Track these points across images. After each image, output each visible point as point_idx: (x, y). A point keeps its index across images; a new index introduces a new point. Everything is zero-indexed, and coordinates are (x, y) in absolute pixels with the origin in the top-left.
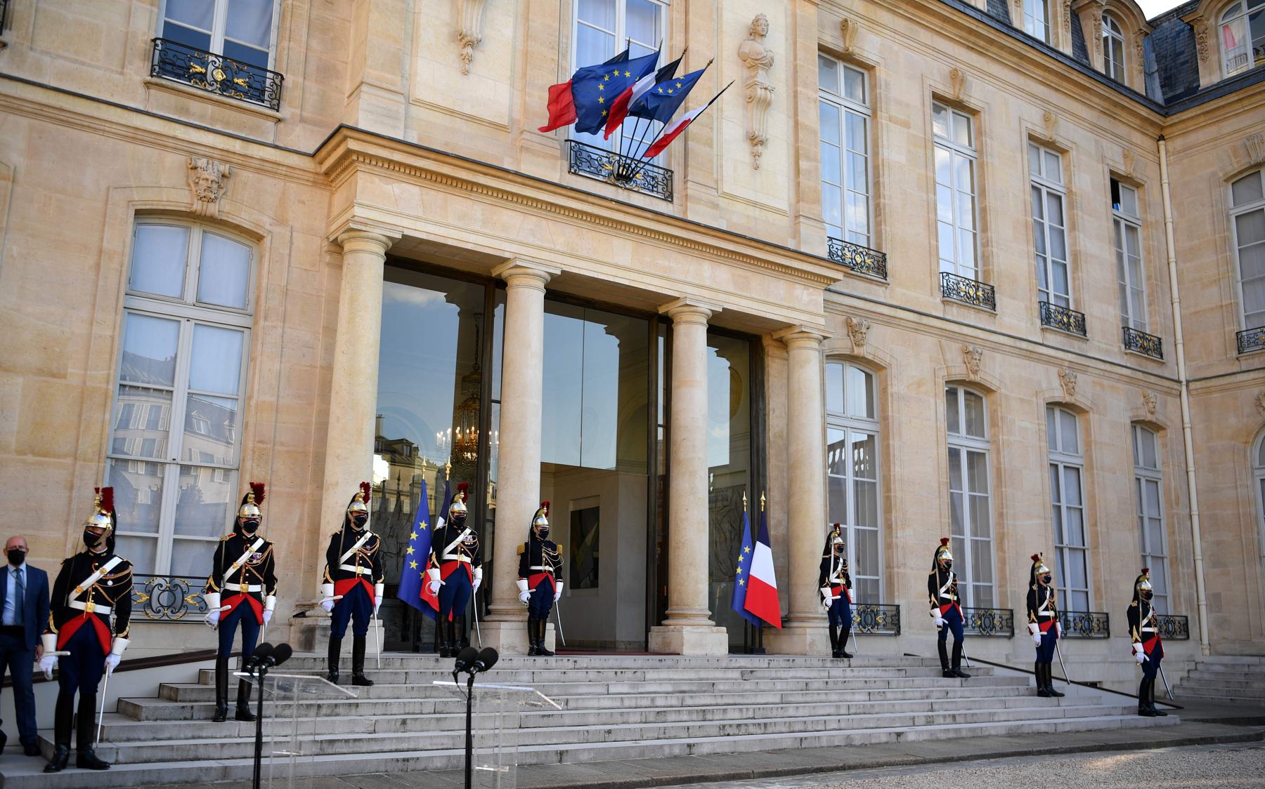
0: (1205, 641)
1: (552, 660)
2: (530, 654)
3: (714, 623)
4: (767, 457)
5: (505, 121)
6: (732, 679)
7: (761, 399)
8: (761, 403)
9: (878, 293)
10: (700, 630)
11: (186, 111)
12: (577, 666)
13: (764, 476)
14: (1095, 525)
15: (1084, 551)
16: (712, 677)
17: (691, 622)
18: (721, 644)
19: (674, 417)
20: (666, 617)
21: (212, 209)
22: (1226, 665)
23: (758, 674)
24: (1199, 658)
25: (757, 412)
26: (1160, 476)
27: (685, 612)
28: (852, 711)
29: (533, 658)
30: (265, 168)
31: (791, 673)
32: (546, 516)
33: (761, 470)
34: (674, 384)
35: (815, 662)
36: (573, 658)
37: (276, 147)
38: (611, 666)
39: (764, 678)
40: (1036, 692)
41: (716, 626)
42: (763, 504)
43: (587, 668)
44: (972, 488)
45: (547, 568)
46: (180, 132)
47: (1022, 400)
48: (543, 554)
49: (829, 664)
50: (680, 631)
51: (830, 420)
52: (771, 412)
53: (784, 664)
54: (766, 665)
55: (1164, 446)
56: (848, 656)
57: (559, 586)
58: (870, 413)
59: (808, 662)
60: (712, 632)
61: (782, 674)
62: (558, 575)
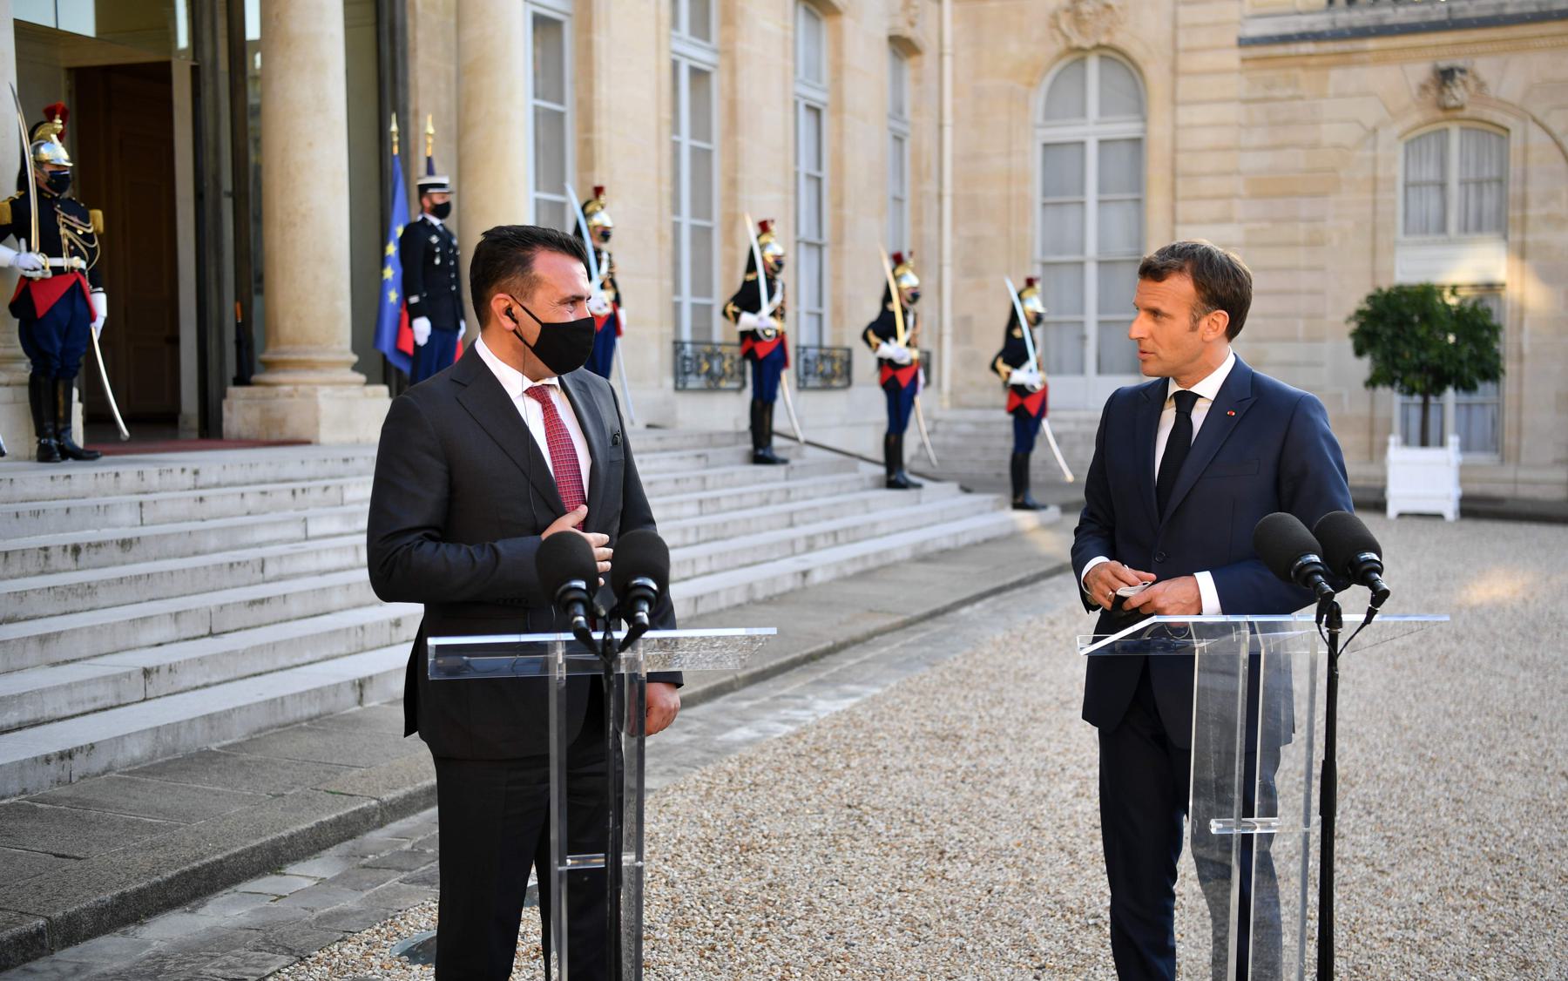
0: (946, 386)
3: (362, 378)
4: (411, 45)
12: (201, 482)
13: (405, 85)
14: (839, 204)
15: (820, 247)
20: (269, 366)
22: (976, 423)
24: (937, 414)
26: (906, 129)
27: (314, 357)
28: (702, 536)
32: (60, 137)
40: (884, 482)
41: (368, 383)
44: (693, 136)
48: (63, 231)
55: (918, 80)
57: (100, 302)
60: (366, 395)
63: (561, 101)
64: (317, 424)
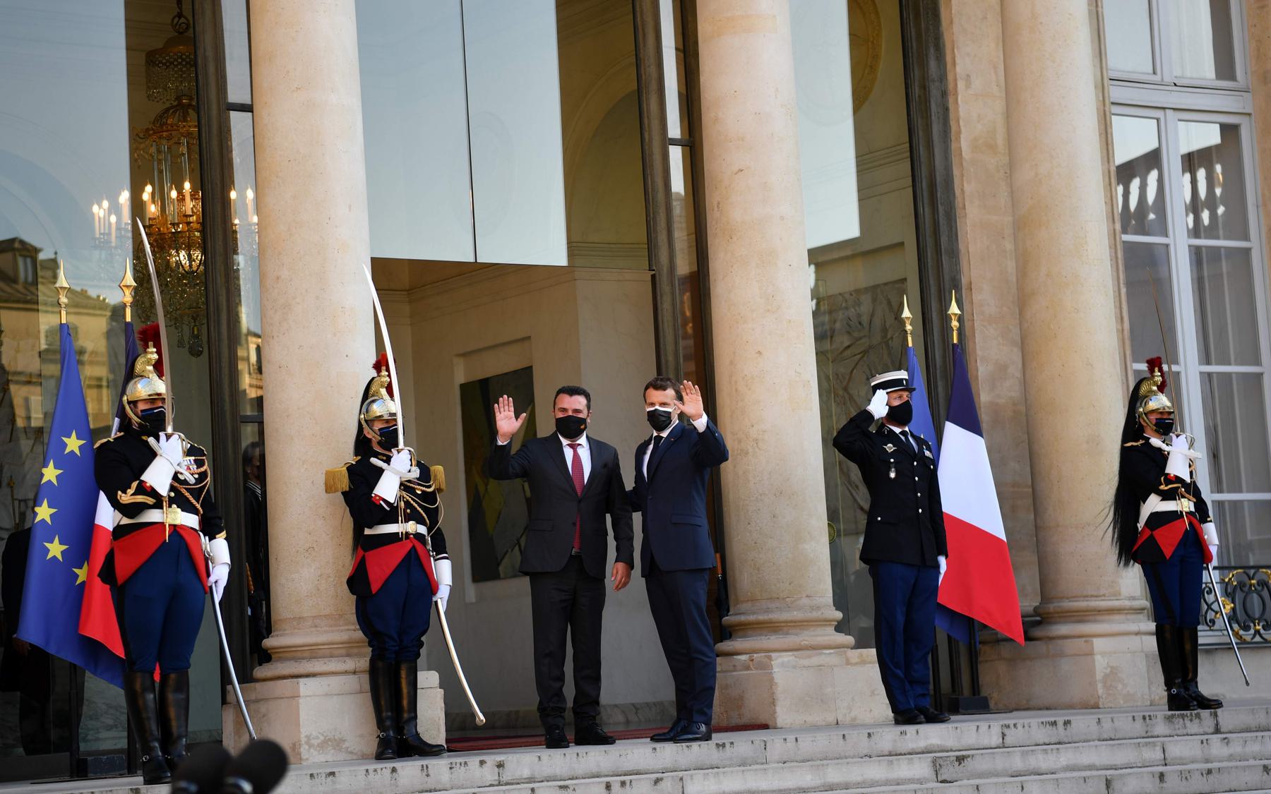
1: (439, 766)
2: (380, 756)
6: (911, 781)
7: (932, 50)
8: (933, 64)
10: (816, 660)
13: (954, 254)
16: (859, 779)
17: (791, 640)
18: (873, 693)
19: (708, 116)
23: (980, 763)
25: (924, 87)
29: (390, 765)
31: (1066, 757)
33: (944, 239)
34: (704, 27)
35: (1124, 724)
36: (492, 758)
38: (595, 770)
39: (996, 774)
42: (955, 324)
43: (531, 780)
45: (412, 527)
49: (1161, 728)
50: (766, 667)
51: (1117, 93)
52: (961, 85)
53: (1041, 734)
54: (995, 740)
56: (1211, 704)
57: (443, 571)
58: (1225, 66)
59: (1107, 724)
60: (848, 663)
61: (1041, 760)
62: (440, 547)
63: (1246, 237)
64: (773, 703)
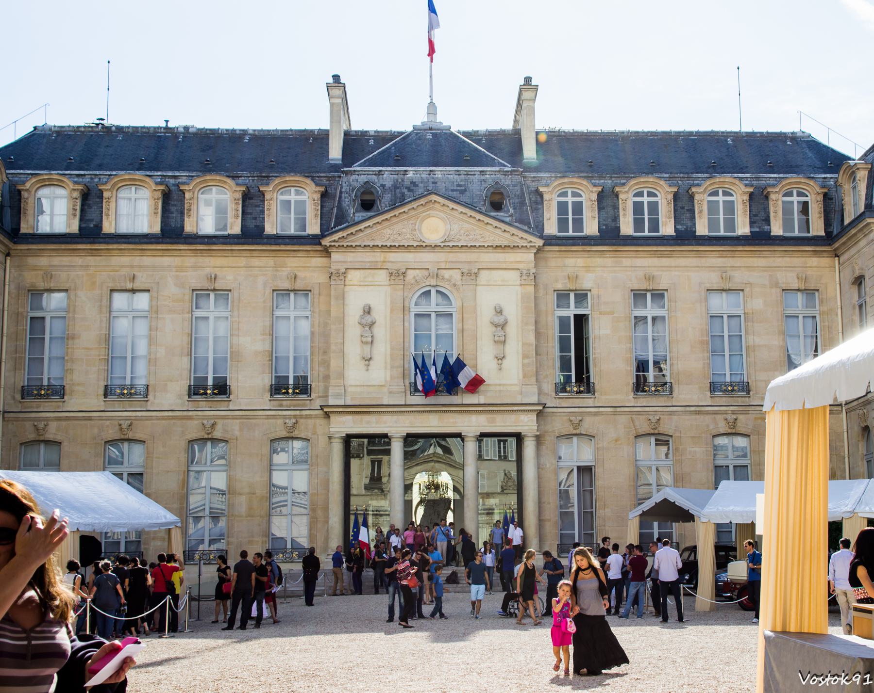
5: (383, 384)
9: (590, 402)
11: (281, 405)
21: (292, 435)
30: (308, 417)
37: (310, 410)
46: (280, 413)
47: (693, 437)
